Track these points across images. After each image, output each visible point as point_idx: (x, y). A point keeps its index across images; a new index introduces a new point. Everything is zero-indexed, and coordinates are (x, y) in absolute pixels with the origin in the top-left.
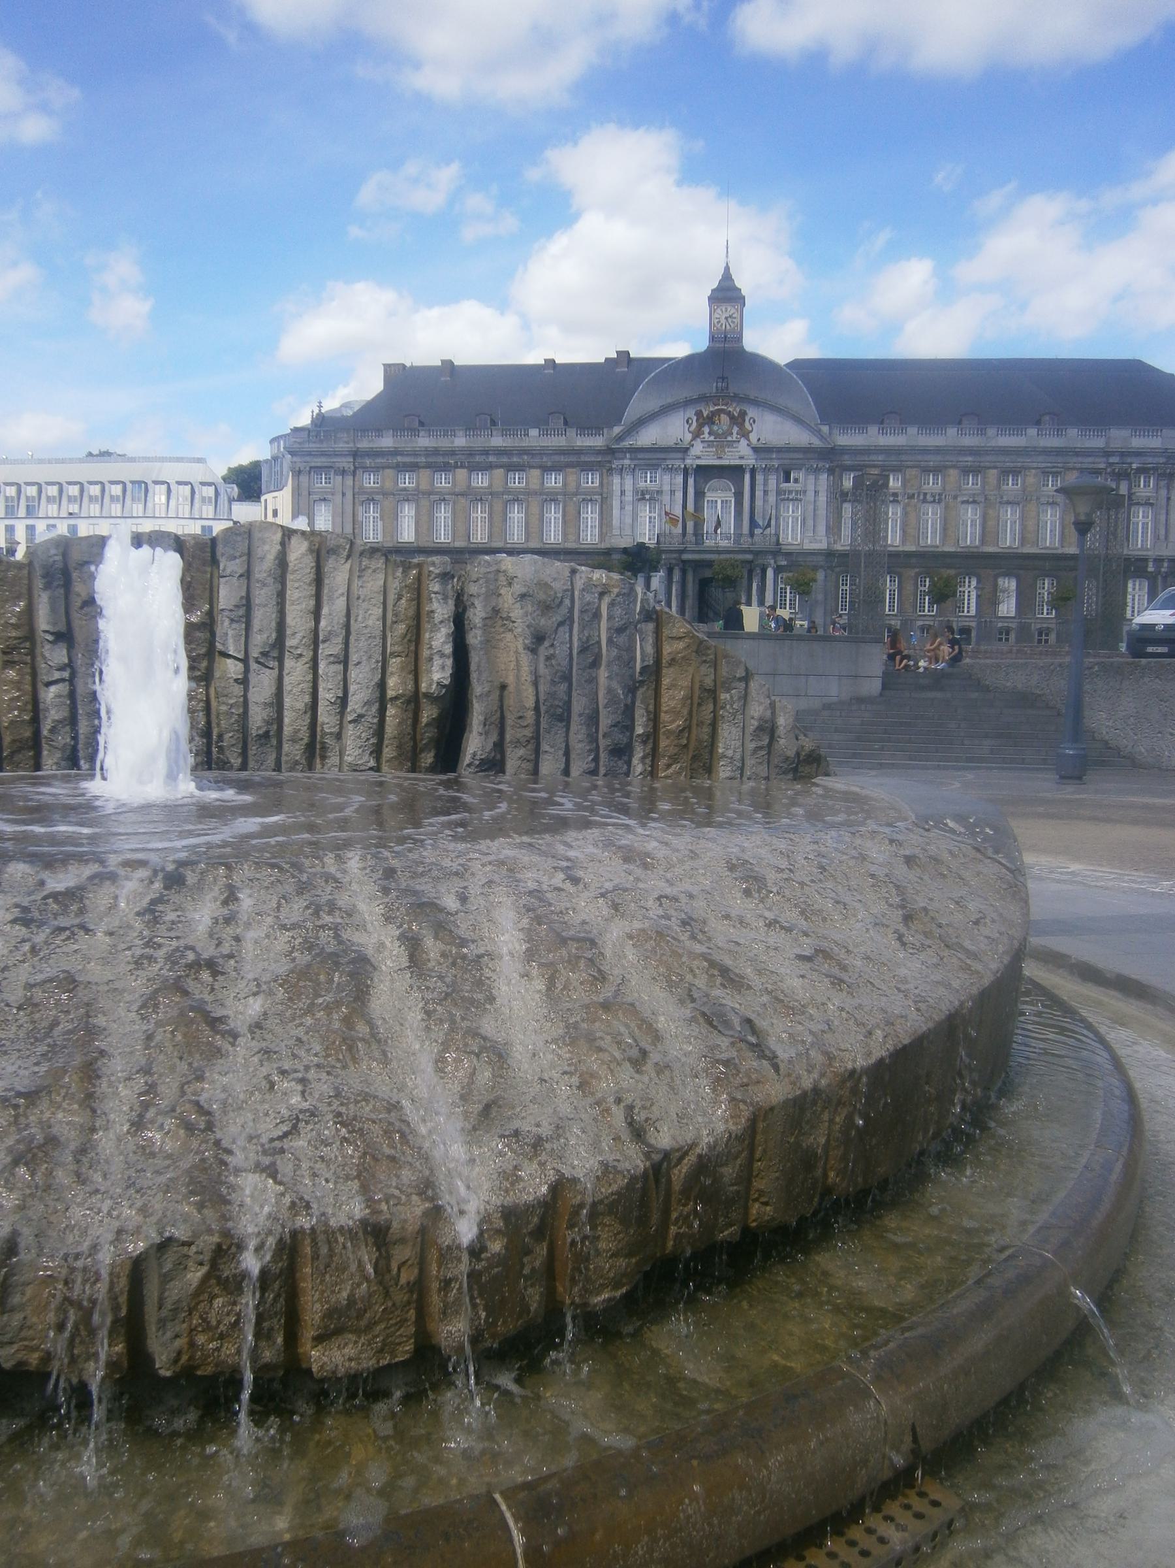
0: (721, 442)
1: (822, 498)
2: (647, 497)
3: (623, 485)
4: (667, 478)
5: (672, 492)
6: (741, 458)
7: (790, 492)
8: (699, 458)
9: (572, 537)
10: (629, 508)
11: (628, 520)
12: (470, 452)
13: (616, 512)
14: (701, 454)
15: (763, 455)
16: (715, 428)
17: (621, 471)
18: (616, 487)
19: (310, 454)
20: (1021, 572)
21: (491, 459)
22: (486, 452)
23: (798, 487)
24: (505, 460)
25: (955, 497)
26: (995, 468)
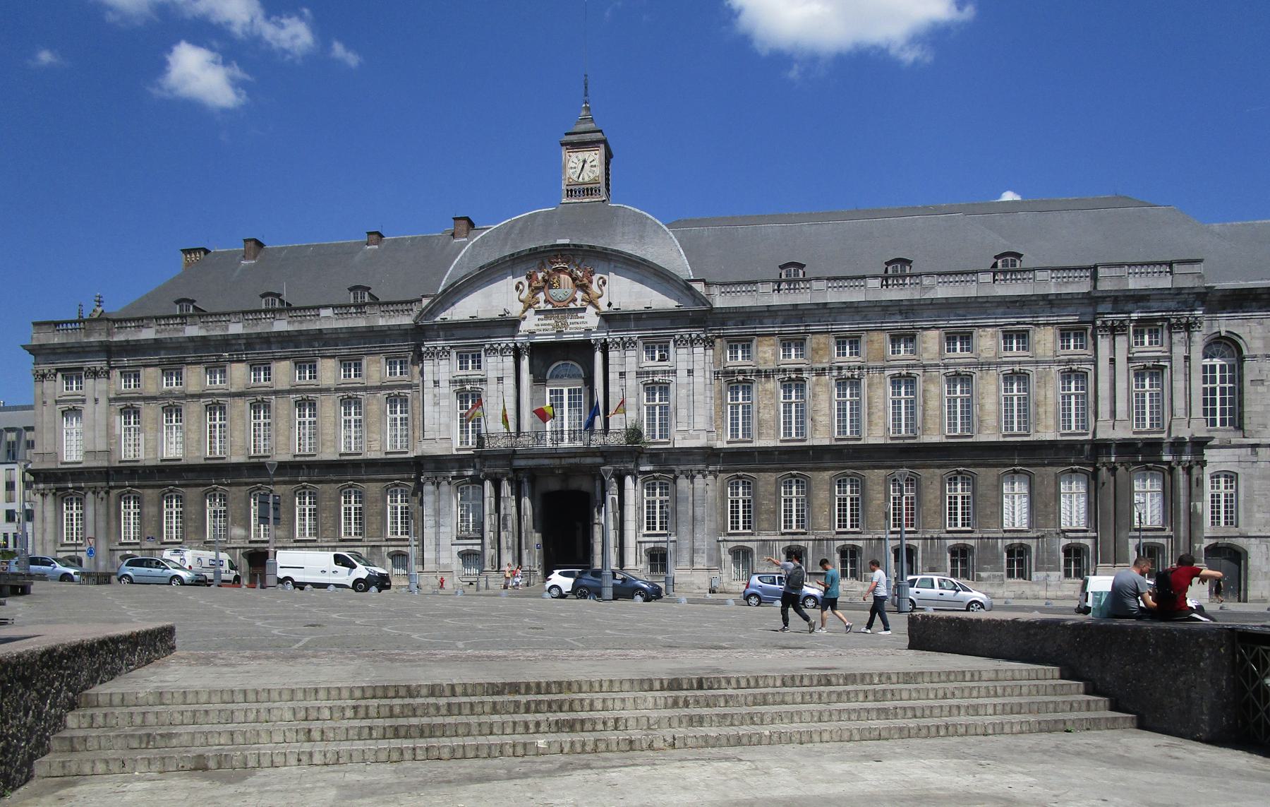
0: (561, 311)
1: (699, 378)
7: (654, 373)
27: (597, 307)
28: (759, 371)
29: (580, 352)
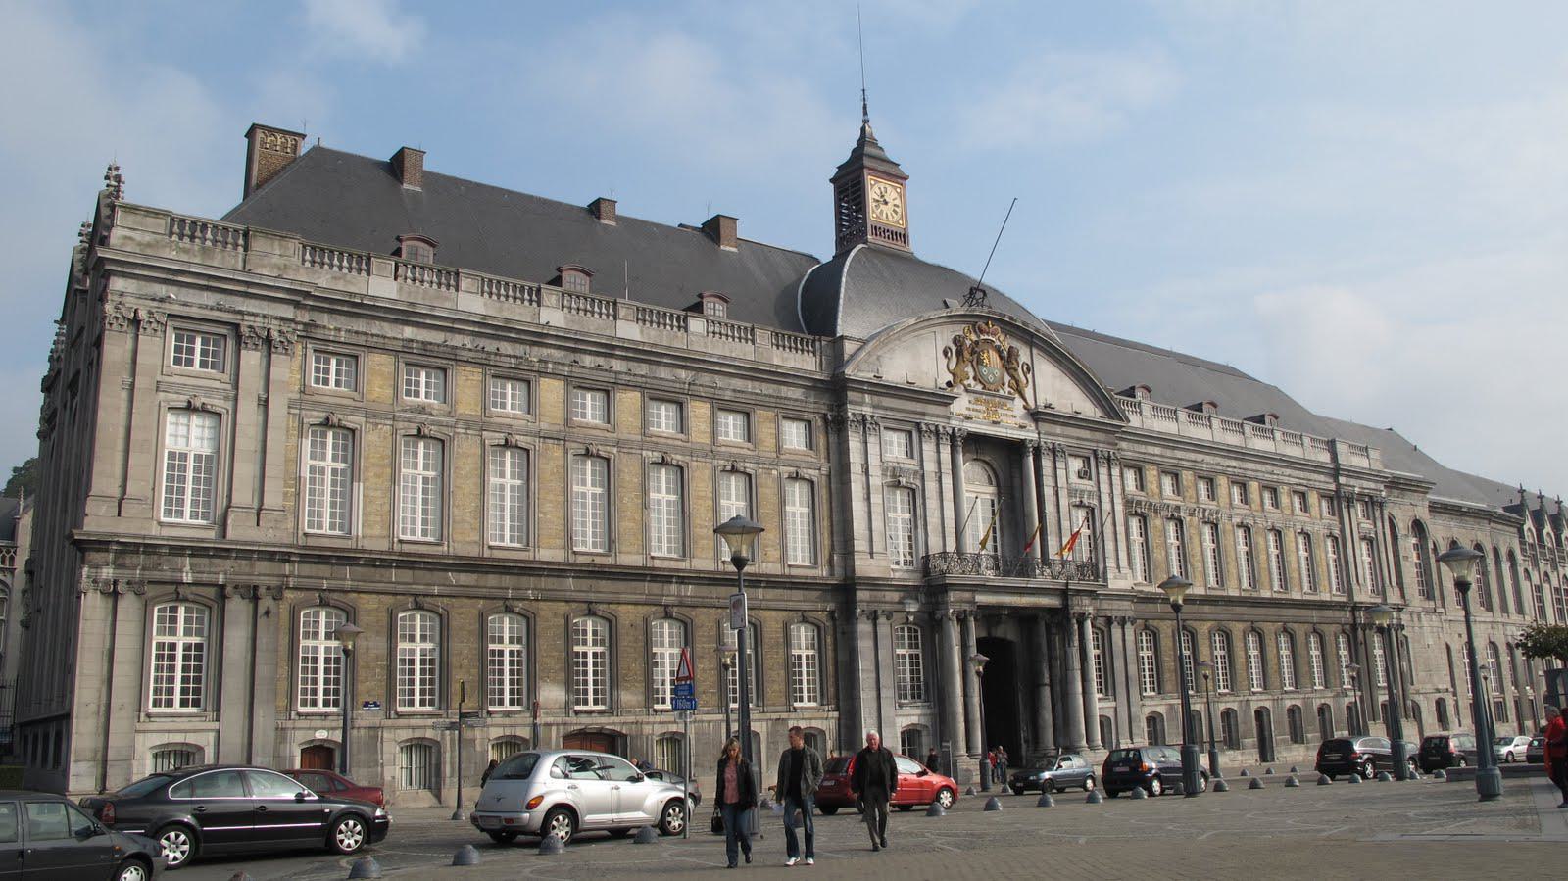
2: (903, 481)
6: (1022, 427)
8: (968, 419)
10: (876, 498)
12: (573, 344)
14: (966, 412)
19: (172, 277)
20: (1295, 626)
21: (618, 365)
22: (609, 349)
24: (643, 369)
25: (1230, 518)
26: (1257, 479)
27: (1025, 400)
28: (1151, 504)
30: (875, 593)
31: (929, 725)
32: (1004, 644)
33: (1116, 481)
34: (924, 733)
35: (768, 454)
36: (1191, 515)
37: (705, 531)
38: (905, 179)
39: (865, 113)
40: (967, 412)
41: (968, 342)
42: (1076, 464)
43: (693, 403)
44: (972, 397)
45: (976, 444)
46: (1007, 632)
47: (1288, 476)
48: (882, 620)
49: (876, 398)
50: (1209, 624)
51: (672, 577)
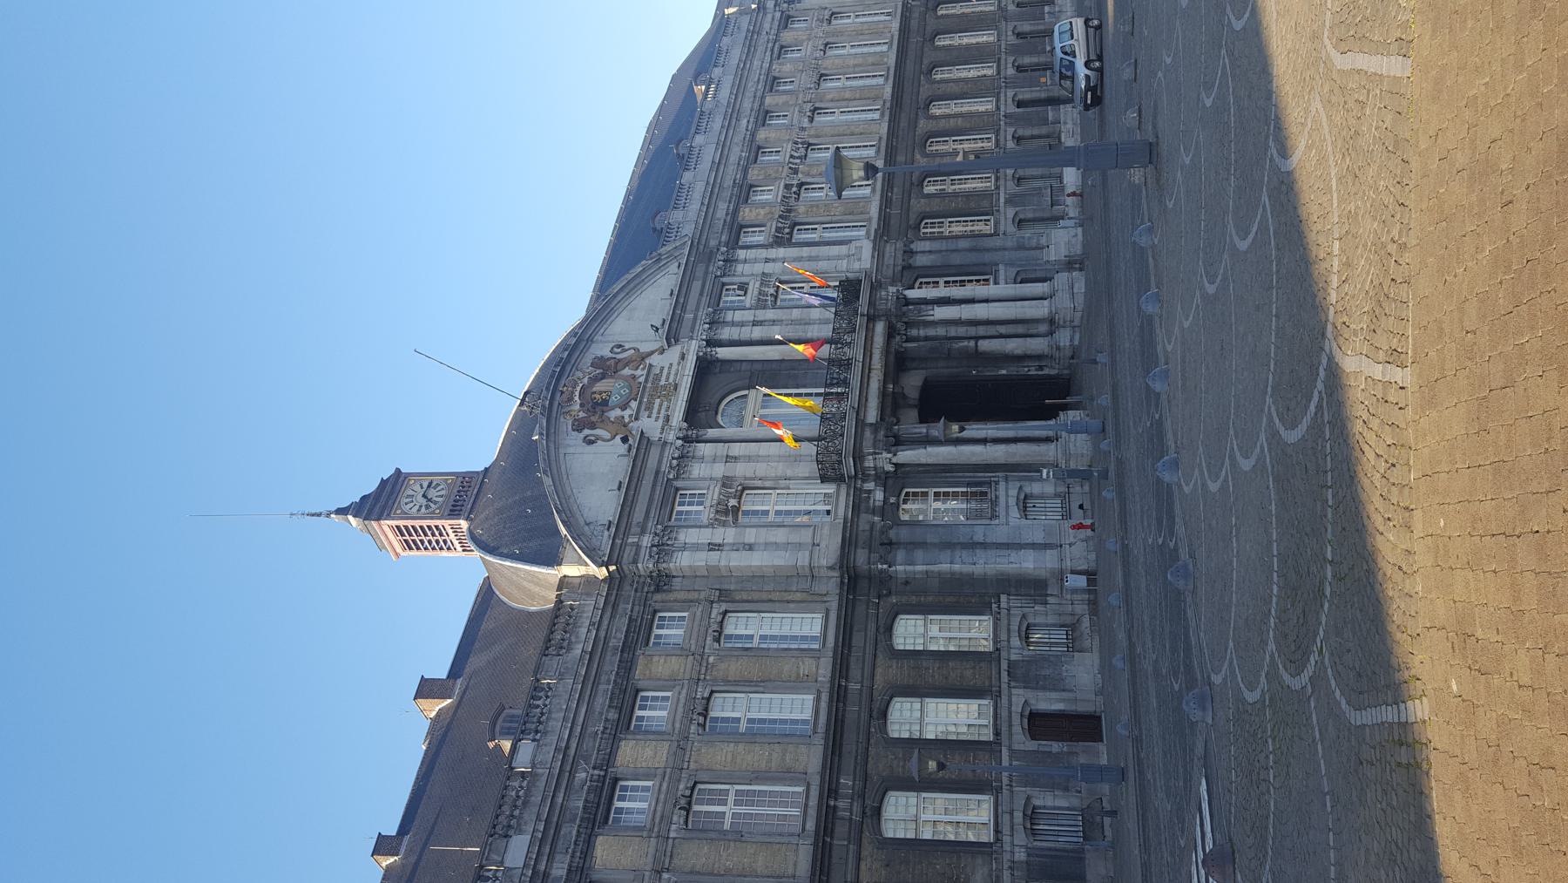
0: (650, 391)
2: (733, 502)
3: (697, 549)
4: (697, 470)
5: (729, 459)
6: (683, 357)
9: (807, 666)
10: (750, 536)
11: (780, 536)
13: (757, 560)
14: (663, 421)
15: (685, 330)
16: (614, 399)
17: (662, 550)
18: (701, 560)
20: (926, 62)
23: (754, 287)
25: (803, 129)
27: (653, 353)
29: (712, 386)
30: (860, 543)
31: (1018, 484)
32: (927, 388)
33: (751, 254)
34: (1027, 489)
35: (689, 666)
36: (796, 171)
37: (775, 755)
38: (398, 471)
39: (319, 515)
40: (661, 421)
41: (582, 414)
42: (729, 298)
43: (618, 763)
44: (644, 414)
45: (699, 413)
46: (913, 382)
47: (759, 63)
48: (892, 534)
49: (635, 529)
50: (918, 156)
51: (828, 806)
